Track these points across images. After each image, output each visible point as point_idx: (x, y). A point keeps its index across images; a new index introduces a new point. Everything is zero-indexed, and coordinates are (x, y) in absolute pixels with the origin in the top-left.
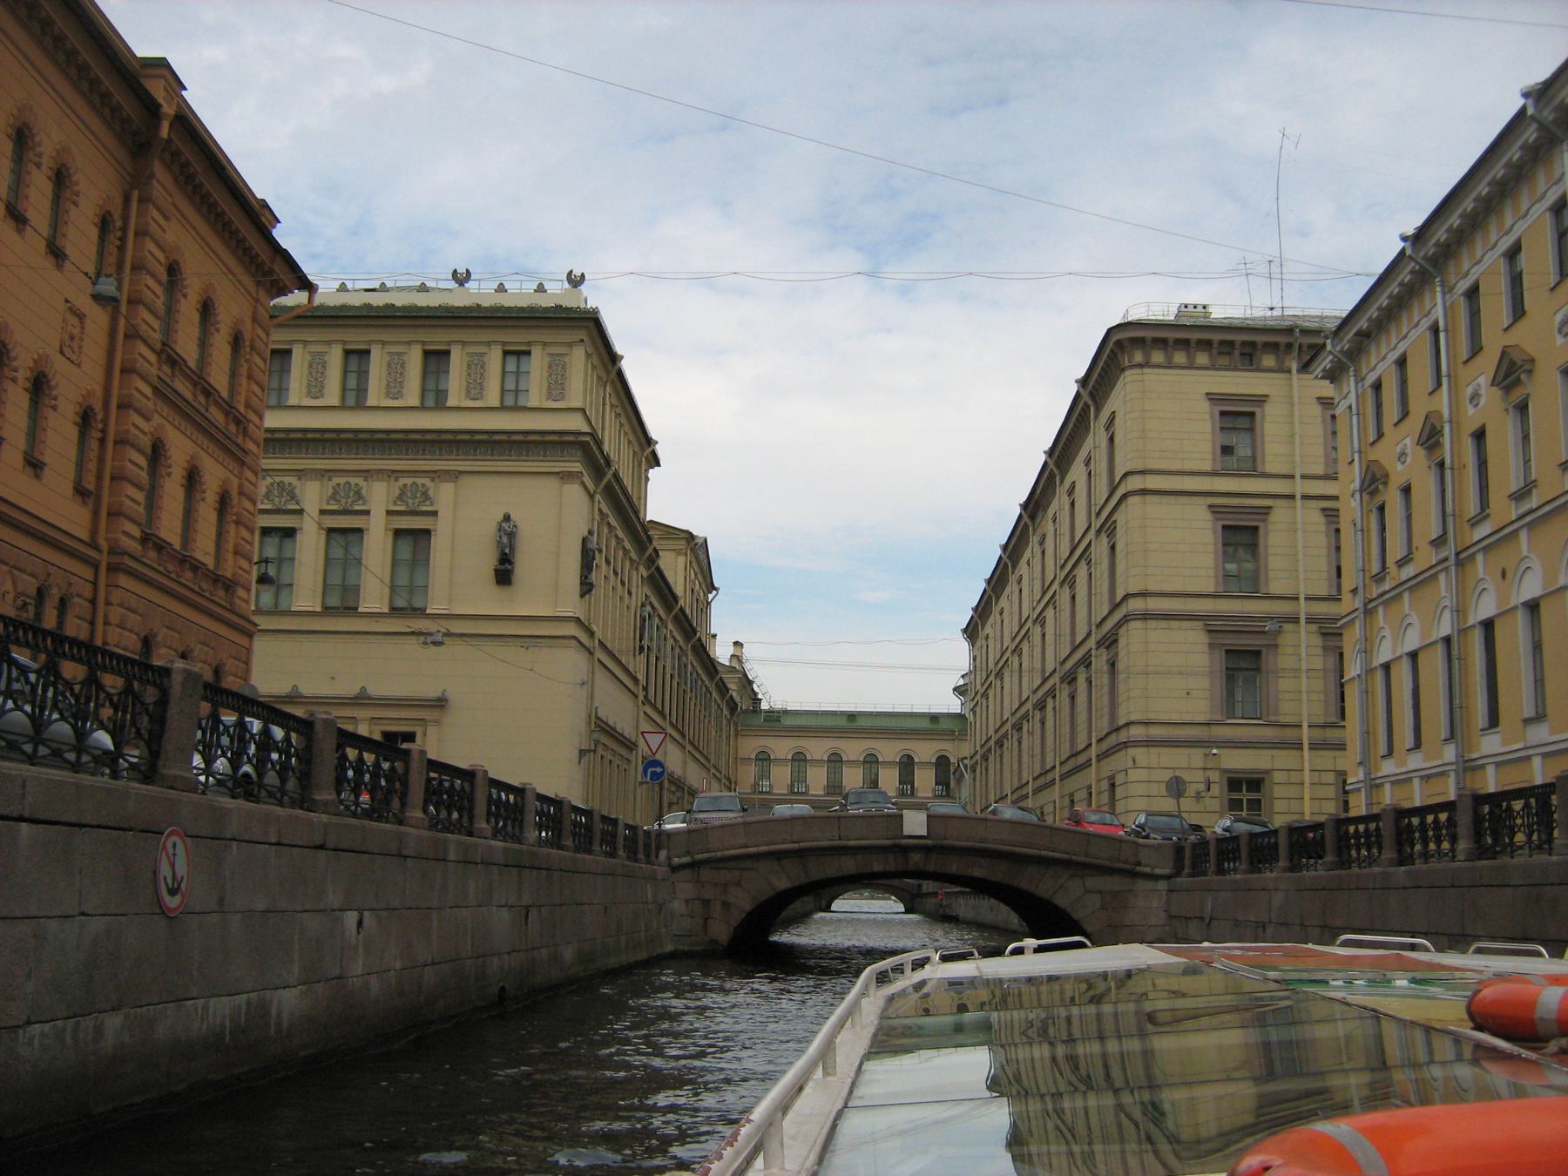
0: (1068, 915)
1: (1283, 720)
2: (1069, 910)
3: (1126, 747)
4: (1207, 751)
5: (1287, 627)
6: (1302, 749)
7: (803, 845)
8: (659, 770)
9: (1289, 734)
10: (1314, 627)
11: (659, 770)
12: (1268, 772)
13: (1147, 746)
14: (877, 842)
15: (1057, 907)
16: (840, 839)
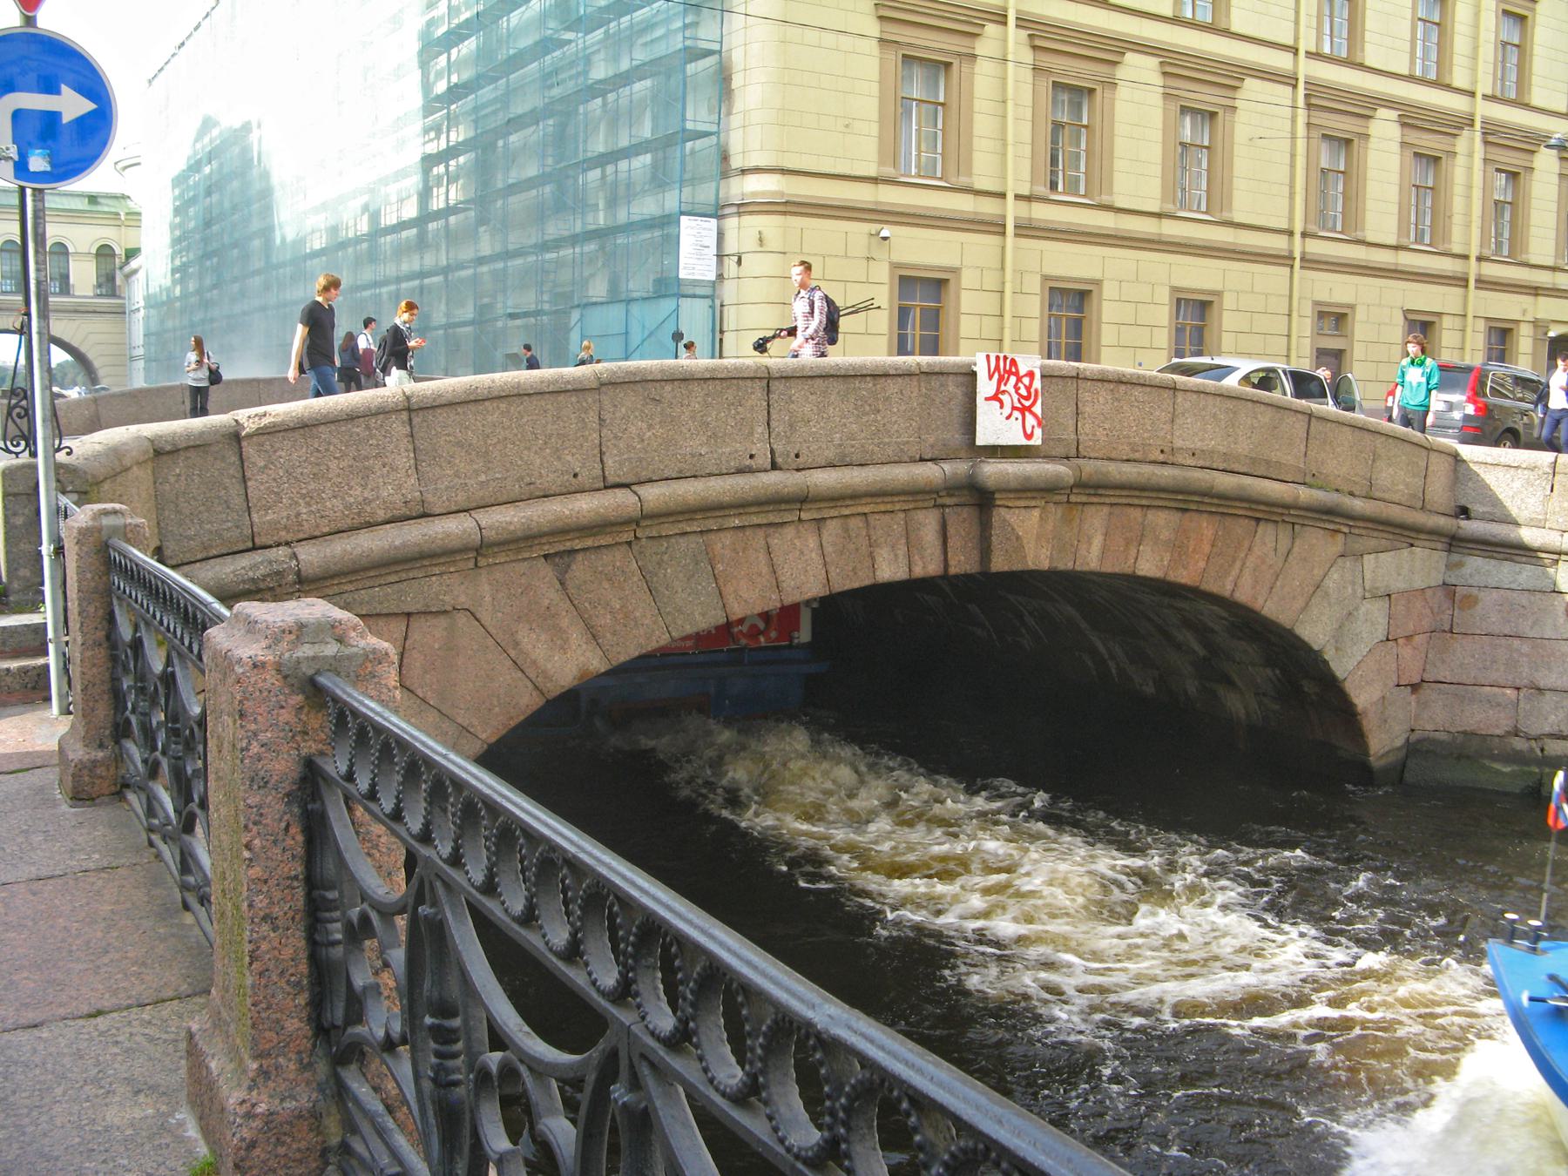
0: (1326, 663)
1: (980, 184)
2: (1329, 655)
3: (739, 214)
4: (874, 227)
5: (991, 29)
6: (1004, 234)
7: (654, 495)
8: (71, 105)
9: (988, 207)
10: (1024, 34)
11: (71, 105)
12: (955, 271)
13: (784, 213)
14: (901, 474)
15: (1303, 642)
16: (774, 466)
